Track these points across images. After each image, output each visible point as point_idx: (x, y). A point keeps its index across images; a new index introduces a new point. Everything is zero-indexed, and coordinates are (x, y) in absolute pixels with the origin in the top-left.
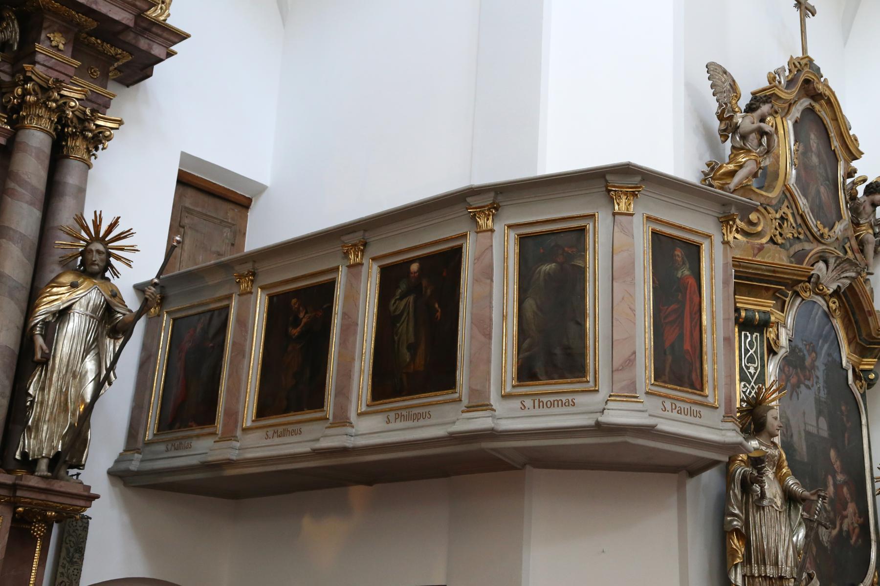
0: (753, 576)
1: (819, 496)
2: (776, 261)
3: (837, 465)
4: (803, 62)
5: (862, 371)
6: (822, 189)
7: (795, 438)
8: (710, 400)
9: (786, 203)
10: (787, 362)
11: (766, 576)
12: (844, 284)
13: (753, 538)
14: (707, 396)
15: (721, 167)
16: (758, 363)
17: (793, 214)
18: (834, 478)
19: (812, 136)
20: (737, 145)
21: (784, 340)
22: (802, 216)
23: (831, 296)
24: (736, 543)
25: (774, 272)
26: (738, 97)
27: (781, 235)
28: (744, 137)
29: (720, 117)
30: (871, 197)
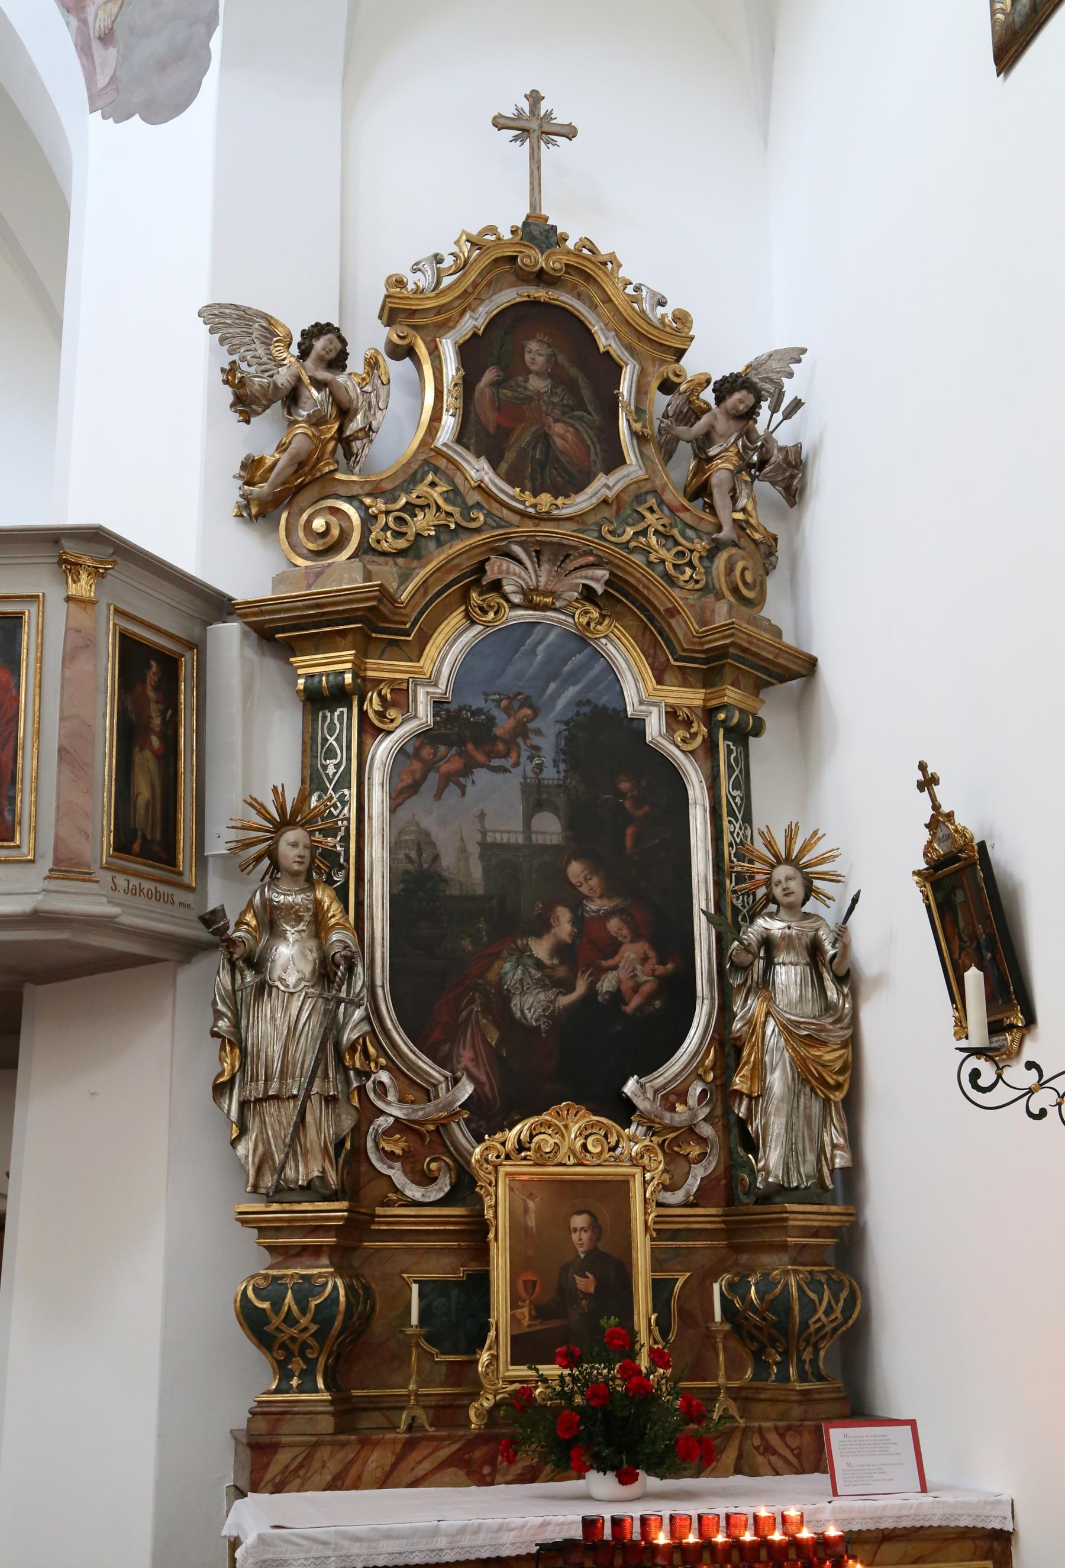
9: (430, 477)
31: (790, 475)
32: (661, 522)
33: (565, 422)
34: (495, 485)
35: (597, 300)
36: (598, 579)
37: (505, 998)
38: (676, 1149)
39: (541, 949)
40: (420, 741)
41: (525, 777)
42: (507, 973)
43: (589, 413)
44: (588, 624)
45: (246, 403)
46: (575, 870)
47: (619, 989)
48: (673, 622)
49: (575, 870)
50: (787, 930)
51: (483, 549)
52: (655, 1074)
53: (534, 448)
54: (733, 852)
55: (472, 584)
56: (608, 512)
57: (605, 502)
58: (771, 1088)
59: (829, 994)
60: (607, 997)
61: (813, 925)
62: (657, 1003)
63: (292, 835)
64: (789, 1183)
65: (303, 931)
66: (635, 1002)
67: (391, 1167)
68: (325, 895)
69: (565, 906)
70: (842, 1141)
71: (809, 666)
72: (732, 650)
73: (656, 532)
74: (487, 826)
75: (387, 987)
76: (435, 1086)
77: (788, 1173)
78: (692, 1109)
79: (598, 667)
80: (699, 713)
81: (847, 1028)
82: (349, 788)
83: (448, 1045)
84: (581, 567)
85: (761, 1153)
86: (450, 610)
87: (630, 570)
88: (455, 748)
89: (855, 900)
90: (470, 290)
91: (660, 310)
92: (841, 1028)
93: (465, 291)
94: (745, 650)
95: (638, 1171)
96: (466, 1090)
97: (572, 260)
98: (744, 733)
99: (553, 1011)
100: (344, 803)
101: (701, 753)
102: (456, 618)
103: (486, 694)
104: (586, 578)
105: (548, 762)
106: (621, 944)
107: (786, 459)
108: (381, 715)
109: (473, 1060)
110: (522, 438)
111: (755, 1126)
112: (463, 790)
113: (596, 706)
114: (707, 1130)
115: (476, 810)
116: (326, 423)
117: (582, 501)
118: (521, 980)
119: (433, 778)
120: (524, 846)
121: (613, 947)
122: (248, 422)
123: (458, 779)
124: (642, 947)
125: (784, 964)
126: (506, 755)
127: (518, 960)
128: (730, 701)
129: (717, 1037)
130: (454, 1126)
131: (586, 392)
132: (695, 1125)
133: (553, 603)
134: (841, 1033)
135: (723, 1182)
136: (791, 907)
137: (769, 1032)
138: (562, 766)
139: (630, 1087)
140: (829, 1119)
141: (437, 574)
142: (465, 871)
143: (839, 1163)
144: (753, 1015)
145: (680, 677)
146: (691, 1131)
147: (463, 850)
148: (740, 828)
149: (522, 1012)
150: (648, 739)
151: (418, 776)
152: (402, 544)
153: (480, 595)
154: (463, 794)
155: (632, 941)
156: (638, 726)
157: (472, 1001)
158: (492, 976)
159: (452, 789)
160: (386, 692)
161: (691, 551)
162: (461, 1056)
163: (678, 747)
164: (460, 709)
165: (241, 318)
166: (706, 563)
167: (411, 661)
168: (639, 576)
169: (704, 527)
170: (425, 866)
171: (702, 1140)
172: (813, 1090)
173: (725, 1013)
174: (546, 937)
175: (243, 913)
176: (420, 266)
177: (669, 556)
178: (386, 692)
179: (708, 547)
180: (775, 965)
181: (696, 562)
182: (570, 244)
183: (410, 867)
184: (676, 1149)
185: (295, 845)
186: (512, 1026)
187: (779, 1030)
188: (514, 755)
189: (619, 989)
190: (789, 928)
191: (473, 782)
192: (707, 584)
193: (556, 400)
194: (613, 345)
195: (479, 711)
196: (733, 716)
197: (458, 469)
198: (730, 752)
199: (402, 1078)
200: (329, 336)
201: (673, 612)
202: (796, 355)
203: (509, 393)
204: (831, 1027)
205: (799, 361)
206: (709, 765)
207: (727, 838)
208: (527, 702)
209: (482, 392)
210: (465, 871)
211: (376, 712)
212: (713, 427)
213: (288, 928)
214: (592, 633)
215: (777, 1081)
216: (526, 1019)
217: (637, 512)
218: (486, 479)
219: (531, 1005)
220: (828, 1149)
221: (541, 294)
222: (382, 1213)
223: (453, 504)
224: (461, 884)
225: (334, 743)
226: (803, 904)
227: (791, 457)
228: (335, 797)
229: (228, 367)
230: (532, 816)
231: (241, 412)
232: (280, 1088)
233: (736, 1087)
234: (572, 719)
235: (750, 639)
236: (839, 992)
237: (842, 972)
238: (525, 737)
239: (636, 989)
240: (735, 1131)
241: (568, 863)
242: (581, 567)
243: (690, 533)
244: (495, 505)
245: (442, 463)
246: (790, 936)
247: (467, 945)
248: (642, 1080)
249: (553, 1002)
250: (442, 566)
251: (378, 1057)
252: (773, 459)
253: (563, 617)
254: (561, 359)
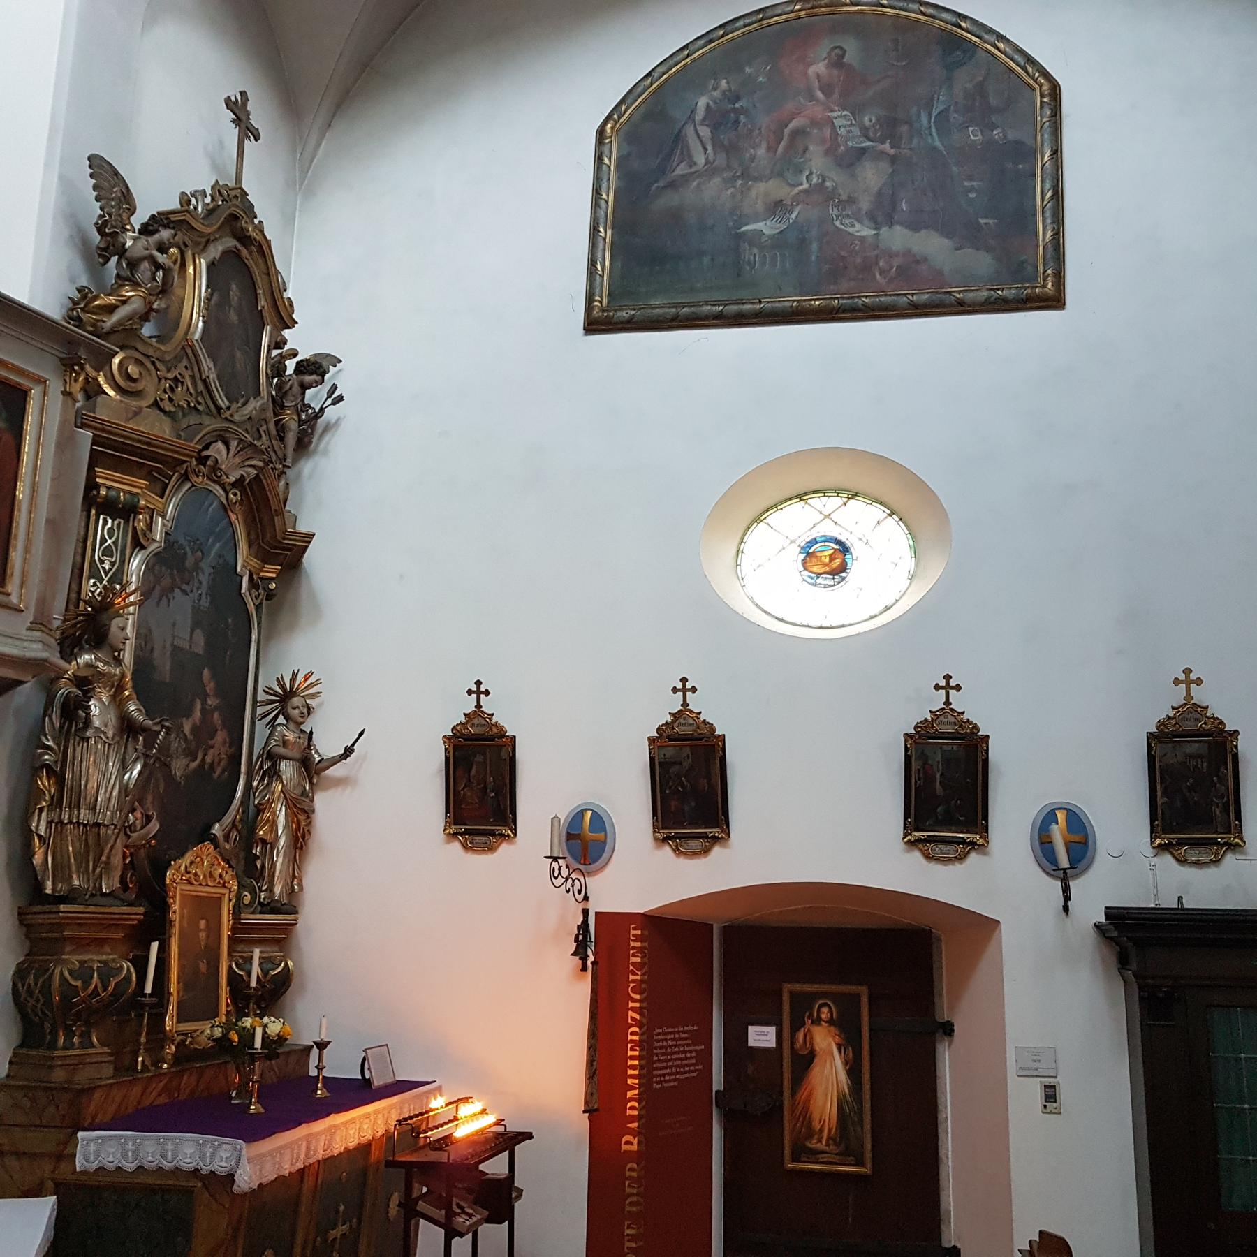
0: (61, 822)
1: (163, 727)
2: (156, 432)
3: (210, 687)
4: (233, 193)
5: (262, 579)
6: (238, 354)
7: (156, 654)
8: (14, 599)
9: (185, 362)
10: (157, 563)
11: (78, 823)
12: (248, 475)
13: (68, 776)
14: (9, 595)
15: (96, 298)
16: (117, 557)
17: (192, 377)
18: (204, 703)
19: (234, 286)
20: (122, 273)
21: (158, 533)
22: (205, 382)
23: (234, 485)
24: (44, 782)
25: (148, 444)
26: (132, 211)
27: (171, 400)
28: (133, 265)
29: (101, 230)
30: (301, 377)
39: (187, 728)
46: (206, 672)
89: (361, 734)
95: (226, 891)
123: (167, 592)
159: (164, 600)
245: (189, 352)
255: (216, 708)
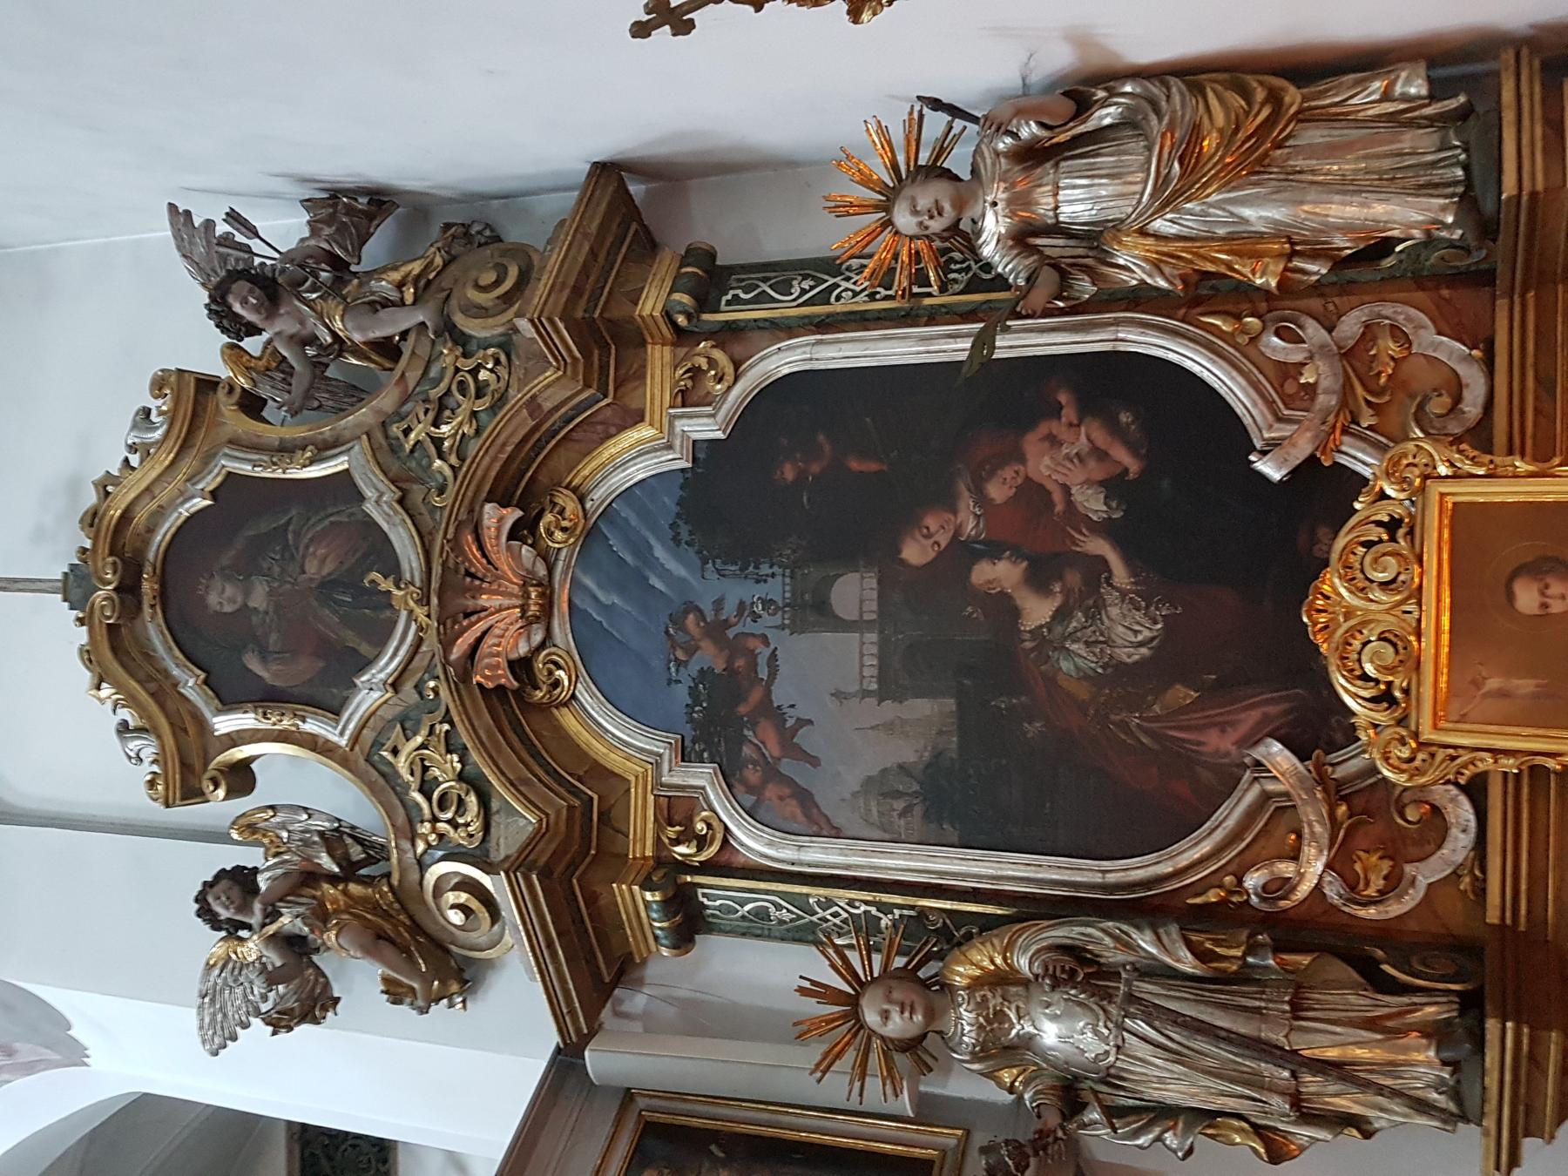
31: (351, 211)
32: (422, 416)
33: (304, 557)
34: (387, 664)
35: (153, 506)
36: (496, 518)
37: (1120, 670)
38: (1383, 380)
39: (1037, 611)
40: (737, 785)
41: (783, 627)
42: (1077, 668)
43: (289, 522)
44: (564, 530)
45: (313, 1004)
46: (915, 552)
47: (1101, 483)
48: (548, 406)
49: (915, 552)
50: (999, 207)
51: (463, 692)
52: (1247, 420)
53: (336, 602)
54: (884, 292)
55: (516, 710)
56: (417, 493)
57: (401, 502)
58: (1276, 222)
59: (1107, 121)
60: (1114, 505)
61: (989, 161)
62: (1125, 418)
63: (871, 1018)
64: (1456, 183)
65: (1018, 1008)
66: (1123, 456)
67: (1413, 882)
68: (961, 973)
69: (970, 570)
70: (1377, 84)
71: (608, 174)
72: (579, 314)
73: (436, 424)
74: (854, 688)
75: (1106, 864)
76: (1266, 797)
77: (1436, 186)
78: (1309, 351)
79: (626, 512)
80: (682, 351)
81: (1168, 89)
82: (808, 895)
83: (1199, 769)
84: (481, 548)
85: (1395, 233)
86: (559, 729)
87: (479, 473)
88: (746, 732)
90: (153, 686)
91: (154, 417)
92: (1168, 97)
93: (152, 695)
94: (577, 291)
96: (1277, 754)
97: (104, 548)
98: (710, 278)
99: (1137, 593)
100: (828, 903)
101: (738, 350)
102: (567, 719)
103: (670, 682)
104: (498, 537)
105: (759, 591)
106: (1028, 479)
107: (329, 221)
108: (702, 842)
109: (1223, 731)
110: (328, 620)
111: (1344, 244)
112: (803, 722)
113: (678, 515)
114: (1350, 326)
115: (832, 704)
116: (322, 904)
117: (403, 540)
118: (1087, 644)
119: (787, 767)
120: (881, 632)
121: (1032, 494)
122: (337, 1000)
124: (1032, 443)
125: (1057, 208)
126: (752, 656)
127: (1055, 649)
128: (659, 306)
129: (1182, 312)
130: (1340, 773)
131: (264, 526)
132: (1340, 348)
133: (539, 584)
134: (1177, 99)
135: (1445, 293)
136: (960, 205)
137: (1174, 230)
138: (765, 569)
139: (1271, 469)
140: (1334, 110)
141: (501, 763)
142: (919, 726)
143: (1418, 88)
144: (1146, 259)
145: (630, 386)
146: (1352, 356)
147: (889, 727)
148: (848, 279)
149: (1141, 644)
150: (720, 435)
151: (787, 791)
152: (472, 800)
153: (537, 688)
154: (810, 722)
155: (1022, 460)
156: (703, 451)
157: (1124, 726)
158: (1083, 692)
159: (803, 738)
160: (672, 832)
161: (457, 370)
162: (1217, 751)
163: (729, 388)
164: (691, 720)
165: (213, 1001)
166: (473, 346)
167: (628, 790)
168: (487, 459)
169: (424, 350)
170: (916, 787)
171: (1369, 332)
172: (1279, 145)
173: (1139, 299)
174: (1018, 602)
175: (1000, 1084)
176: (132, 754)
177: (466, 405)
178: (672, 832)
179: (450, 344)
180: (1058, 222)
181: (470, 364)
182: (88, 544)
183: (918, 811)
184: (1383, 380)
185: (885, 1015)
186: (1166, 663)
187: (1172, 211)
188: (752, 643)
189: (1101, 483)
190: (995, 204)
191: (792, 706)
192: (499, 346)
193: (277, 569)
194: (200, 486)
195: (693, 691)
196: (680, 303)
197: (374, 713)
198: (736, 300)
199: (1257, 848)
200: (210, 899)
201: (532, 404)
202: (180, 218)
203: (273, 637)
204: (1166, 120)
205: (188, 213)
206: (756, 335)
207: (862, 304)
208: (677, 620)
209: (275, 675)
210: (919, 726)
211: (700, 849)
212: (292, 337)
213: (1014, 1032)
214: (576, 525)
215: (1260, 213)
216: (1153, 639)
217: (412, 451)
218: (382, 676)
219: (1130, 631)
220: (1390, 107)
221: (148, 587)
222: (1498, 913)
223: (418, 722)
224: (940, 733)
225: (748, 907)
226: (956, 178)
227: (324, 212)
228: (821, 913)
229: (270, 1029)
230: (836, 617)
231: (325, 1009)
232: (1282, 1094)
233: (1273, 283)
234: (699, 552)
235: (557, 287)
236: (1104, 104)
237: (1069, 106)
238: (726, 624)
239: (1101, 455)
240: (1351, 273)
241: (903, 562)
242: (481, 548)
243: (433, 373)
244: (414, 663)
246: (1009, 202)
247: (1033, 729)
248: (1258, 444)
249: (1123, 594)
250: (491, 757)
251: (1220, 887)
252: (325, 246)
253: (560, 564)
254: (225, 560)
255: (981, 499)
